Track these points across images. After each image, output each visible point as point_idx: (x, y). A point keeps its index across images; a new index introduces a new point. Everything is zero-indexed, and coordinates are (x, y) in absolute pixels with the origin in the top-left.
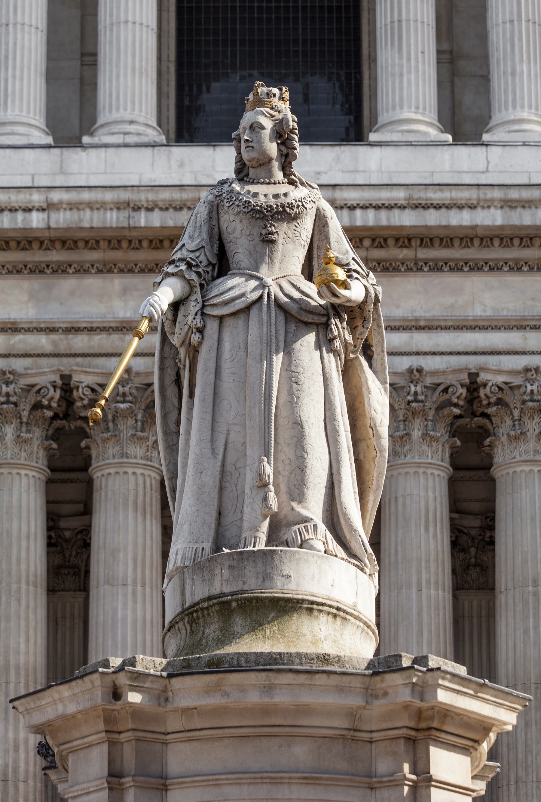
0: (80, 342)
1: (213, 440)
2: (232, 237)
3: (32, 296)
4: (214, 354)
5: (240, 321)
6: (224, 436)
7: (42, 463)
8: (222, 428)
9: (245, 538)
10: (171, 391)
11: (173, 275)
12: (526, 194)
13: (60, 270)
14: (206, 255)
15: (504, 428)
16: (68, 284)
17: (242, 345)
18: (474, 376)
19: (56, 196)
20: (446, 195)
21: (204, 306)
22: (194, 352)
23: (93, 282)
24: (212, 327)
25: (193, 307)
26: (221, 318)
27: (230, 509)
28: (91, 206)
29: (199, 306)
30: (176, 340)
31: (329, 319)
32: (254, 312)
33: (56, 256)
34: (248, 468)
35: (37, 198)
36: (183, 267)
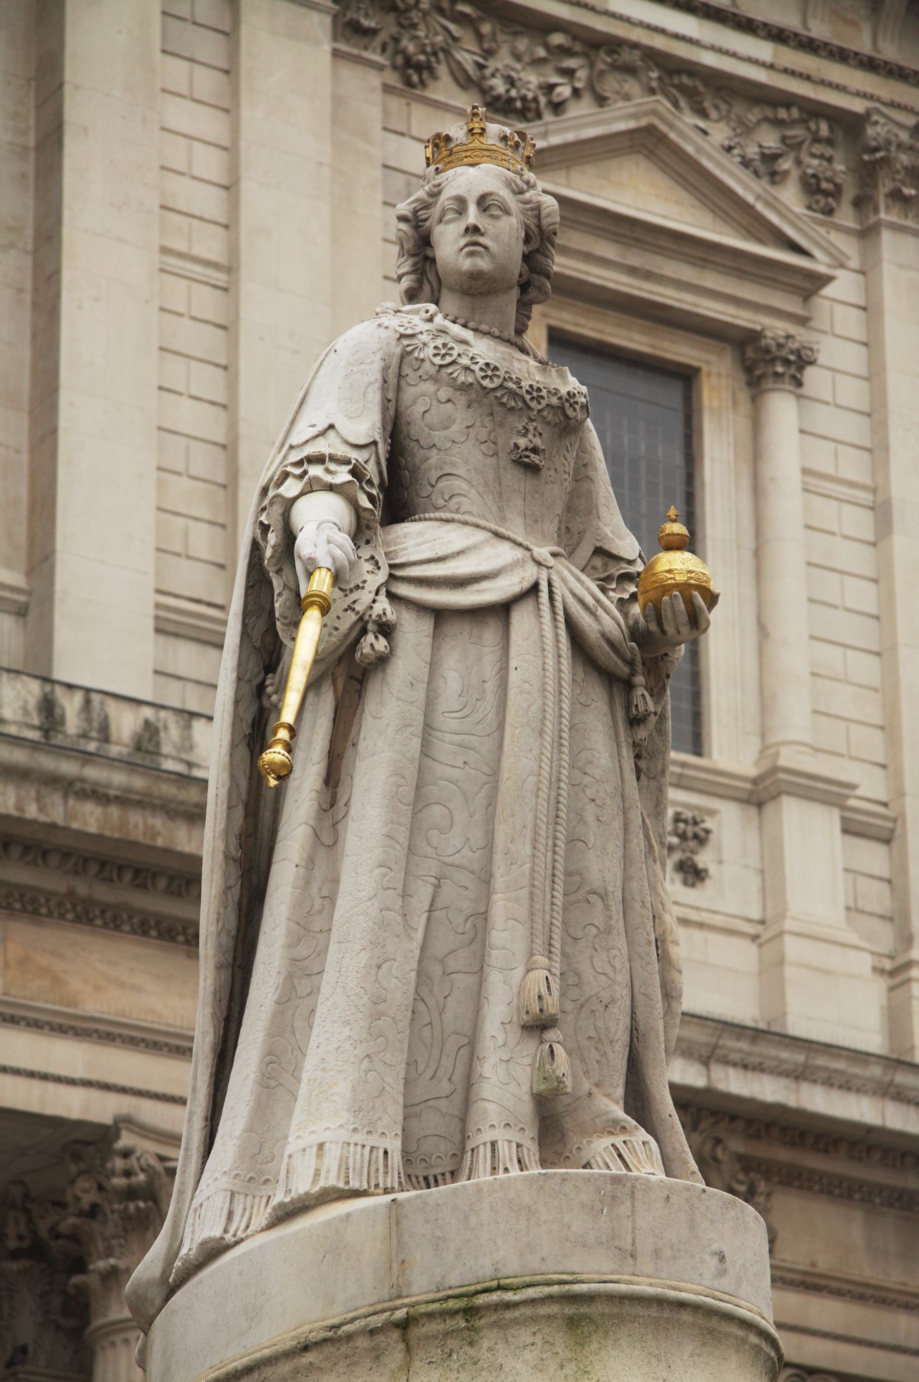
1: (405, 895)
2: (438, 436)
4: (420, 695)
5: (490, 634)
6: (430, 889)
9: (493, 1144)
11: (331, 488)
14: (378, 463)
17: (491, 687)
21: (391, 576)
24: (414, 632)
27: (421, 1067)
29: (382, 576)
31: (633, 674)
32: (521, 619)
34: (494, 978)
36: (343, 475)
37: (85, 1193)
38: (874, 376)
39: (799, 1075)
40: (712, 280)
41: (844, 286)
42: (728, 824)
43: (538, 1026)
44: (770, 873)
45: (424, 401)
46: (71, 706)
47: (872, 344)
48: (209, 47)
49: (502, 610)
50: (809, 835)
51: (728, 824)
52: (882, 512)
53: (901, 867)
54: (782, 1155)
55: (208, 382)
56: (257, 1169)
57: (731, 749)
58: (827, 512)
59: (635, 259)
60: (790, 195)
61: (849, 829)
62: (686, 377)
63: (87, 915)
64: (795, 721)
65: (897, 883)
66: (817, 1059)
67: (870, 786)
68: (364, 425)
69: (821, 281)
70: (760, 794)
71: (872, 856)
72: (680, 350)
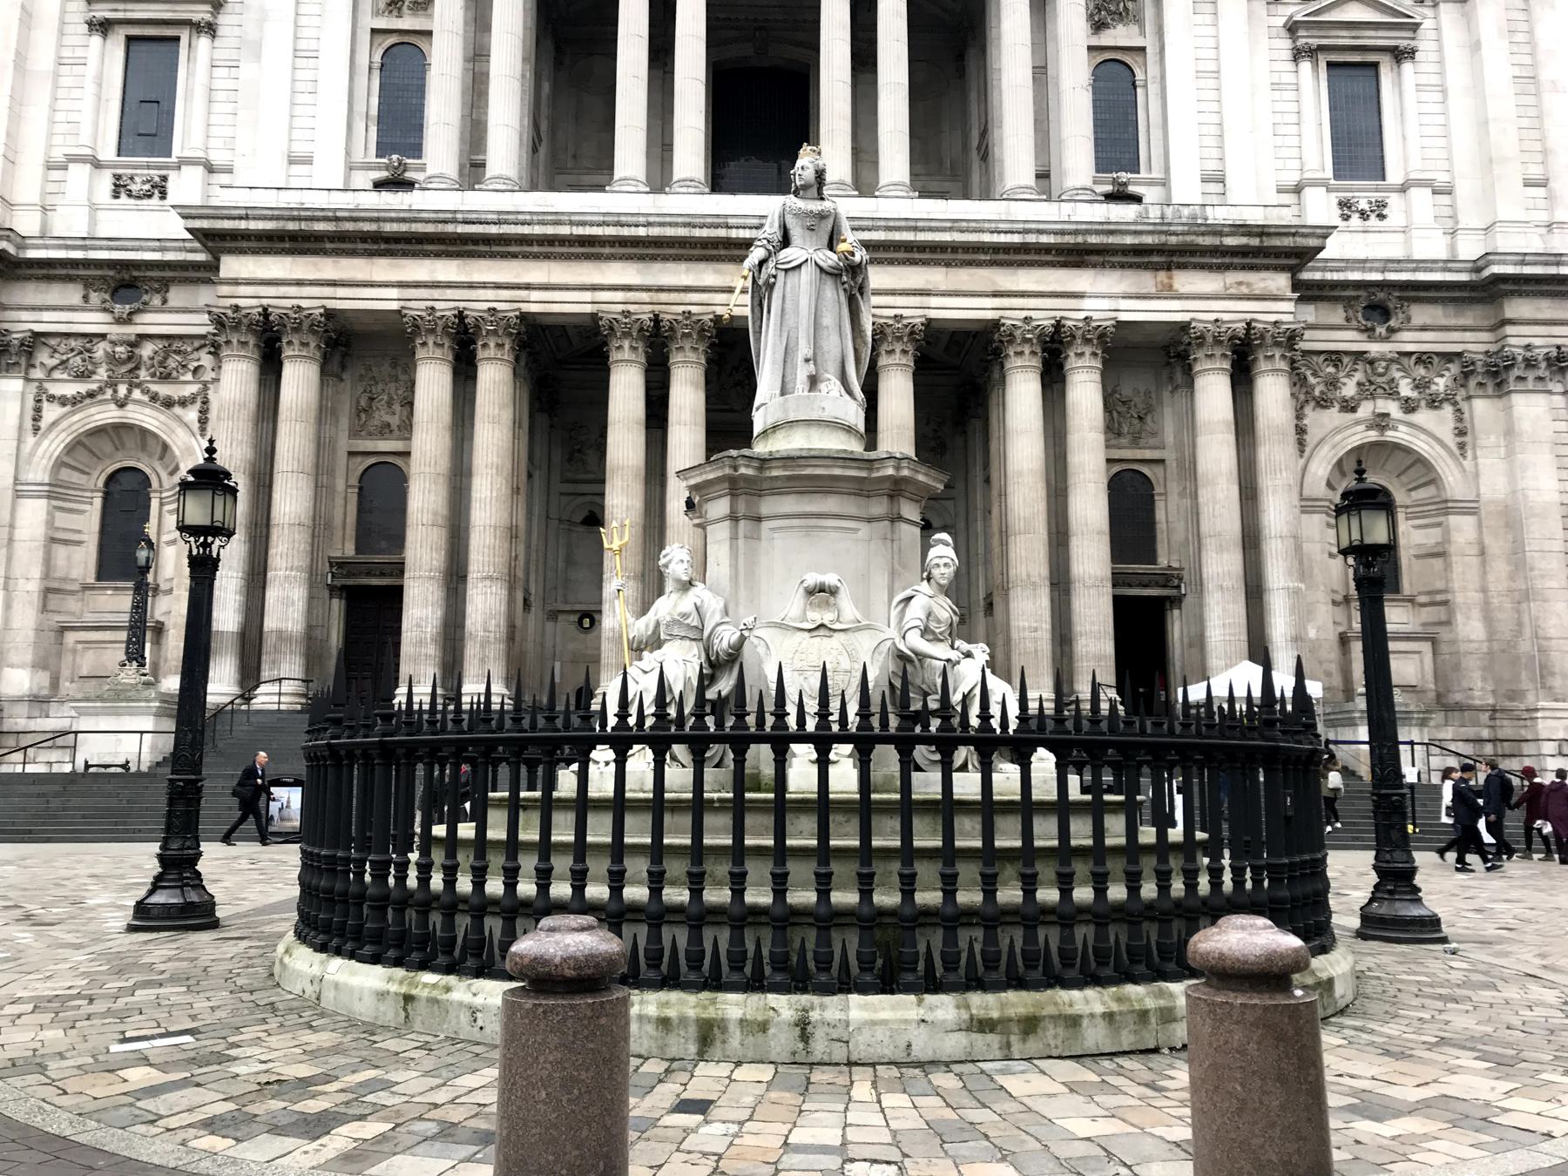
0: (664, 297)
3: (638, 272)
5: (796, 273)
7: (643, 360)
8: (785, 329)
10: (757, 309)
12: (898, 224)
13: (654, 258)
16: (657, 266)
19: (651, 219)
22: (771, 287)
23: (671, 265)
25: (771, 264)
26: (786, 270)
28: (670, 224)
30: (761, 282)
33: (651, 251)
35: (642, 219)
37: (1186, 339)
38: (1440, 50)
39: (1414, 270)
40: (1381, 33)
41: (1427, 24)
42: (1394, 200)
43: (807, 360)
44: (1408, 212)
48: (1209, 8)
49: (799, 266)
50: (1420, 196)
51: (1394, 200)
52: (1444, 92)
53: (1454, 200)
54: (1413, 294)
57: (1394, 175)
58: (1424, 96)
59: (1354, 33)
61: (1434, 193)
62: (1375, 65)
66: (1421, 264)
67: (1442, 178)
69: (1418, 25)
70: (1403, 189)
71: (1445, 199)
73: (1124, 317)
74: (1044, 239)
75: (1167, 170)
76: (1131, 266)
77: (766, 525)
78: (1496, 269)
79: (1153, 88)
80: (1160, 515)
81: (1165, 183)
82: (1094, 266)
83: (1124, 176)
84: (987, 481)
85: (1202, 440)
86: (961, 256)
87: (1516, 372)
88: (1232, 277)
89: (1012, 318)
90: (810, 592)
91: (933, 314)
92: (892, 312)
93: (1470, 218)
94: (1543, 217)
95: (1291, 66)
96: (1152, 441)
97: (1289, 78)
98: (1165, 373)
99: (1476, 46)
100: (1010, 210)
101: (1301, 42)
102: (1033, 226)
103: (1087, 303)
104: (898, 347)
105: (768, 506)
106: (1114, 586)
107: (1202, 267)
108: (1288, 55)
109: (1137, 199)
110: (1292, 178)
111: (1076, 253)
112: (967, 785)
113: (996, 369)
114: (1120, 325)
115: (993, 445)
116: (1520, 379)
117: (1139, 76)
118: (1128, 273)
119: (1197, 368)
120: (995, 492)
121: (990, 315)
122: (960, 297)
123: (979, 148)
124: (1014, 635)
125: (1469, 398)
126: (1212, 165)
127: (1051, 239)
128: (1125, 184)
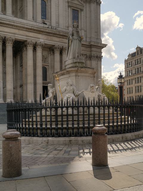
15: (8, 42)
18: (5, 37)
20: (4, 19)
38: (86, 11)
40: (79, 6)
41: (85, 6)
45: (74, 32)
46: (52, 27)
47: (86, 9)
52: (86, 17)
55: (58, 12)
56: (69, 58)
60: (83, 2)
63: (53, 36)
64: (82, 26)
65: (86, 34)
67: (85, 29)
68: (72, 33)
71: (86, 33)
72: (78, 9)
73: (46, 43)
74: (35, 28)
75: (51, 20)
76: (47, 35)
77: (79, 77)
78: (92, 44)
79: (49, 7)
80: (48, 74)
81: (51, 22)
82: (42, 34)
83: (44, 20)
84: (21, 66)
85: (55, 63)
86: (21, 29)
87: (92, 58)
88: (61, 39)
89: (29, 40)
90: (91, 87)
91: (16, 38)
92: (10, 36)
93: (88, 36)
94: (96, 37)
95: (67, 8)
96: (47, 62)
97: (67, 10)
98: (49, 52)
99: (91, 11)
100: (28, 22)
101: (69, 5)
102: (33, 26)
103: (41, 40)
104: (10, 42)
105: (79, 74)
106: (43, 84)
107: (57, 37)
108: (67, 6)
109: (46, 24)
110: (67, 25)
111: (39, 32)
112: (48, 113)
113: (25, 48)
114: (45, 44)
115: (24, 61)
116: (93, 59)
117: (47, 4)
118: (46, 36)
119: (55, 52)
120: (24, 68)
121: (25, 39)
122: (21, 35)
123: (20, 10)
124: (28, 91)
125: (87, 61)
126: (57, 21)
127: (36, 29)
128: (45, 21)
